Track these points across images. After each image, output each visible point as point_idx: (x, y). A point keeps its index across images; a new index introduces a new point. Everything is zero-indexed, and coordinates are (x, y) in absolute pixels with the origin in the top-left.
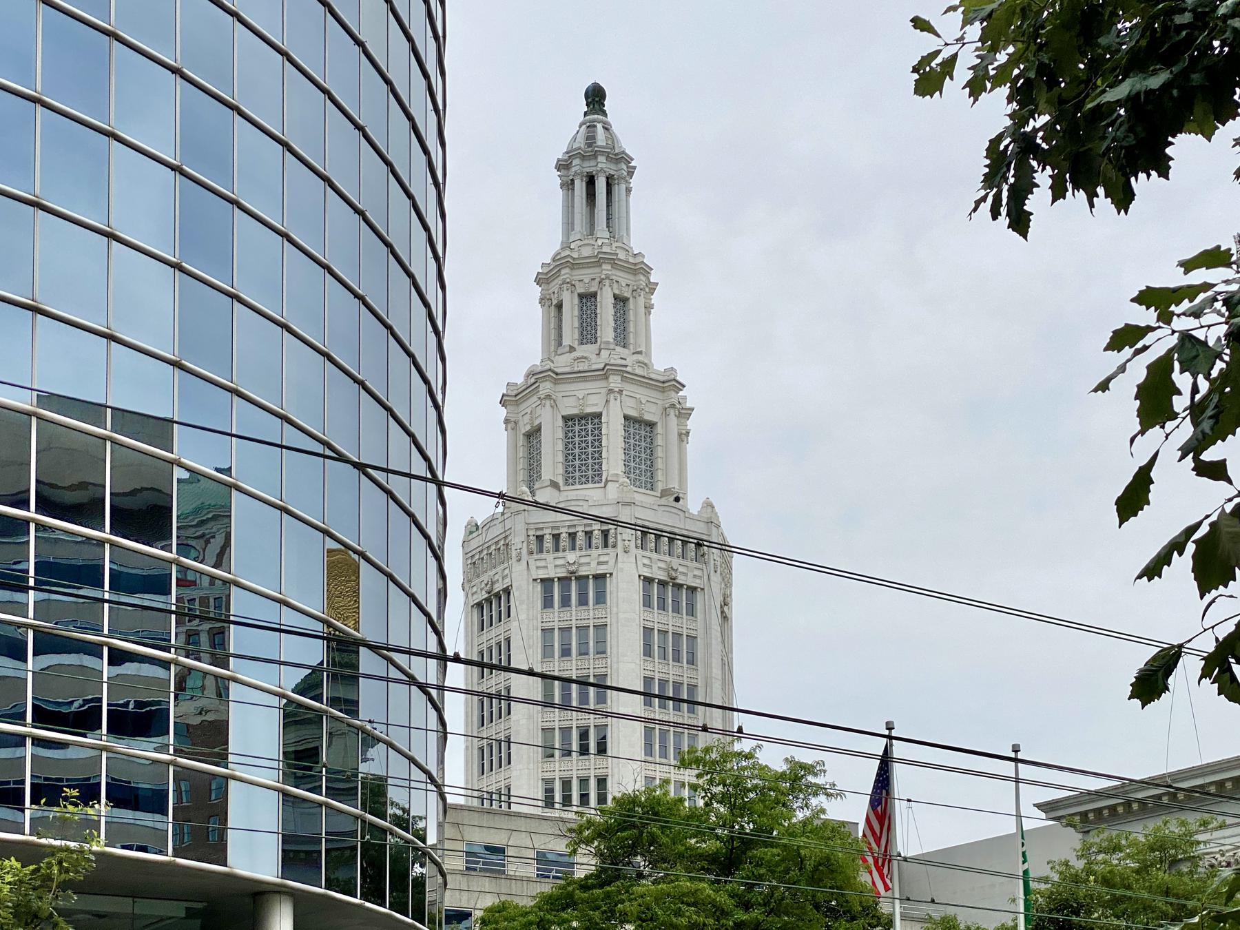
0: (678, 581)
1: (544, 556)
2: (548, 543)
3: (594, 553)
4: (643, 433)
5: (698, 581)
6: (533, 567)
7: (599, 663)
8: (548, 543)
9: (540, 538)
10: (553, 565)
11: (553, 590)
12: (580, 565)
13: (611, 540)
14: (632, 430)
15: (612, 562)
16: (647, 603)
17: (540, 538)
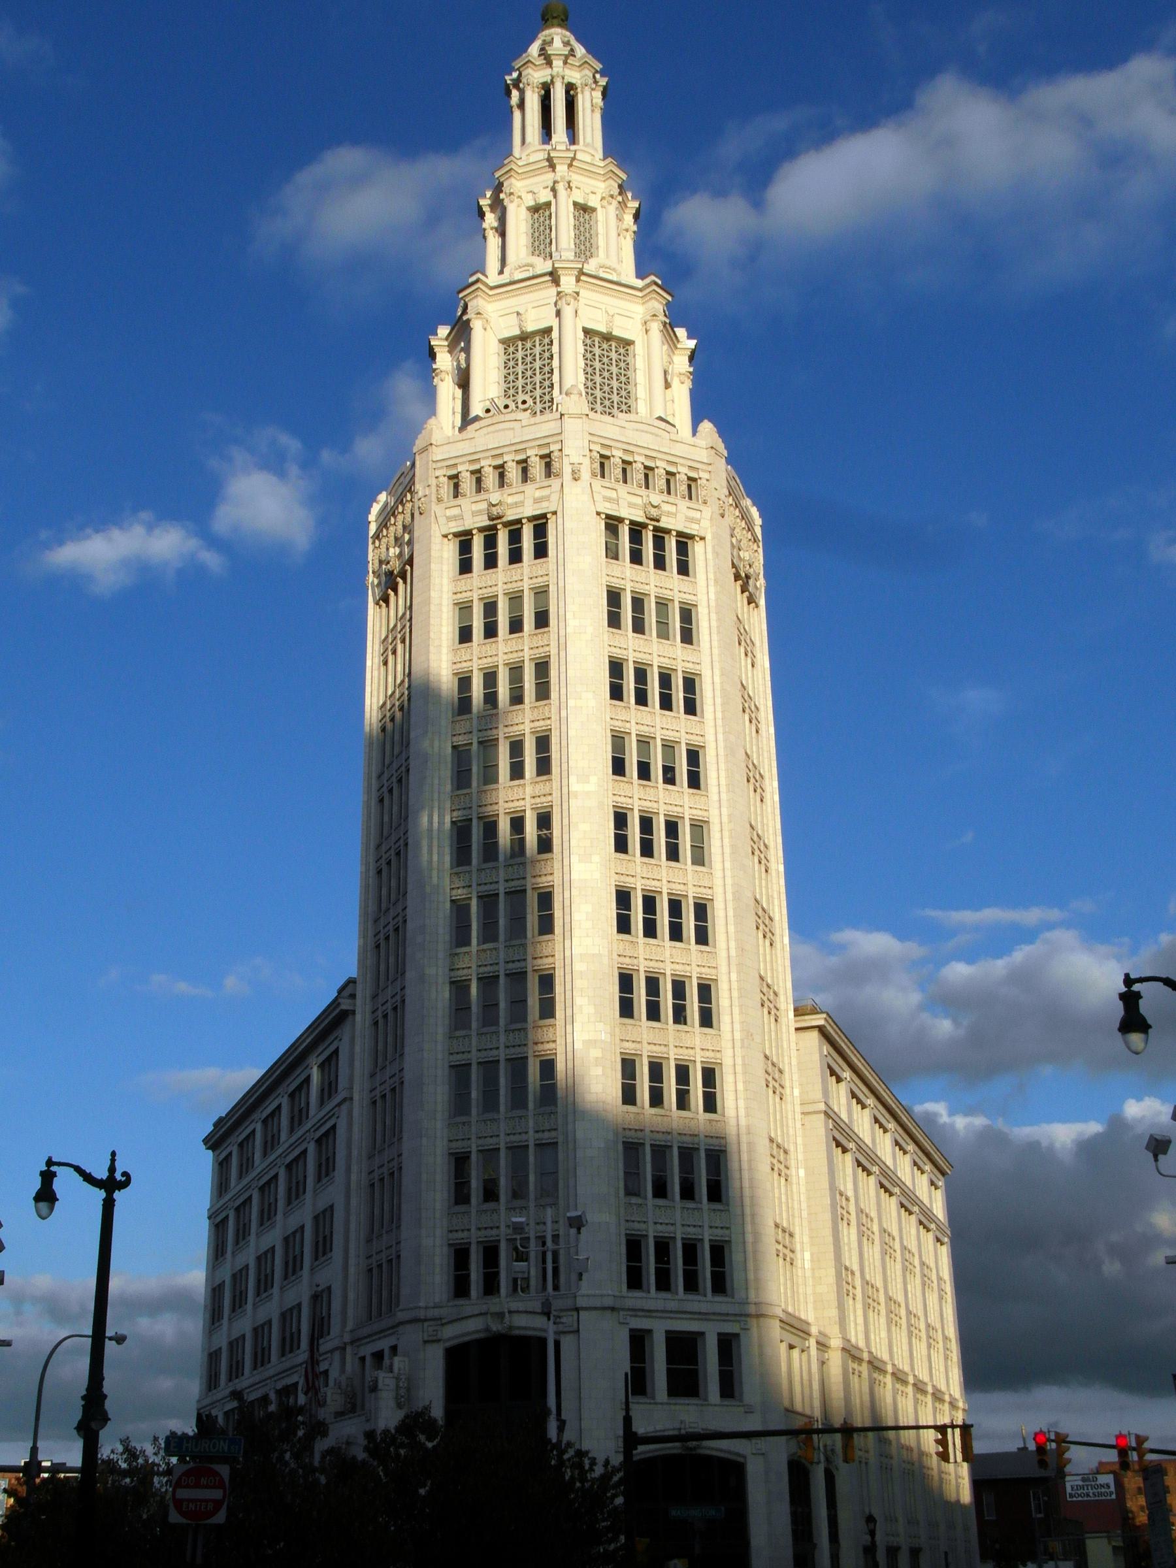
0: (662, 524)
1: (460, 500)
2: (467, 483)
3: (529, 488)
4: (614, 355)
5: (696, 526)
6: (442, 520)
7: (539, 641)
8: (467, 483)
9: (455, 479)
10: (471, 513)
11: (477, 548)
12: (511, 506)
13: (555, 465)
14: (597, 351)
15: (555, 497)
16: (612, 553)
17: (455, 479)
